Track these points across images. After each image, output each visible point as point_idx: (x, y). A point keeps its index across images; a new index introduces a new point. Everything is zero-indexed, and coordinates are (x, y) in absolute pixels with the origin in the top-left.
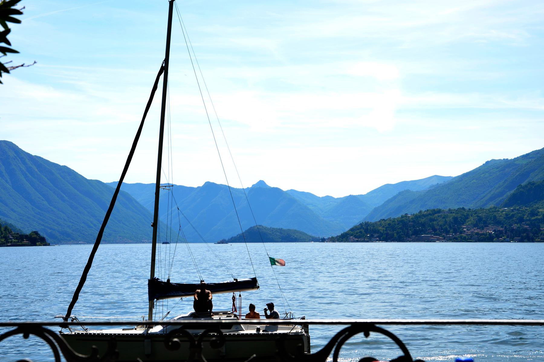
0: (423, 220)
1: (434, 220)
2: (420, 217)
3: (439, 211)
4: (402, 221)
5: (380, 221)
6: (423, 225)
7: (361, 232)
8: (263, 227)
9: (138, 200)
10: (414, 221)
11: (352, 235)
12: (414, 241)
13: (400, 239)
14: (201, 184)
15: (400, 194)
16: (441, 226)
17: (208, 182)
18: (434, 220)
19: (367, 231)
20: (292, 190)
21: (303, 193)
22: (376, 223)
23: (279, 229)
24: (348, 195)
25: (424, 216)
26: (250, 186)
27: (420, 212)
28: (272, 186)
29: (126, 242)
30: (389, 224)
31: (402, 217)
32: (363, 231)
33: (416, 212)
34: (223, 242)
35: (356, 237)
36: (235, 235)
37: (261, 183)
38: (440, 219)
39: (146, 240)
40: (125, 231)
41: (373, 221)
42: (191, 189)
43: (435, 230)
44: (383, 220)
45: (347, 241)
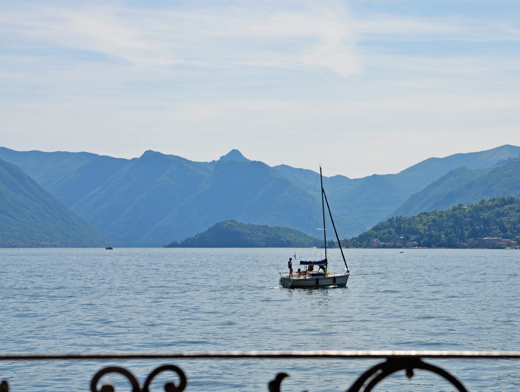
0: (485, 215)
1: (503, 215)
2: (481, 209)
3: (512, 201)
4: (454, 216)
5: (419, 216)
6: (486, 222)
7: (390, 232)
8: (236, 223)
9: (34, 178)
10: (472, 217)
11: (376, 237)
12: (471, 247)
13: (450, 245)
14: (138, 155)
15: (451, 173)
16: (514, 224)
17: (150, 151)
18: (503, 215)
19: (399, 230)
20: (283, 166)
21: (300, 171)
22: (413, 219)
23: (262, 226)
24: (371, 174)
25: (489, 208)
26: (217, 159)
27: (482, 202)
28: (252, 160)
29: (13, 245)
30: (434, 221)
31: (454, 209)
32: (393, 230)
33: (476, 202)
34: (174, 245)
35: (382, 240)
36: (193, 236)
37: (235, 153)
38: (512, 213)
39: (48, 243)
40: (13, 227)
41: (409, 215)
42: (123, 161)
43: (504, 230)
44: (425, 213)
45: (368, 246)
